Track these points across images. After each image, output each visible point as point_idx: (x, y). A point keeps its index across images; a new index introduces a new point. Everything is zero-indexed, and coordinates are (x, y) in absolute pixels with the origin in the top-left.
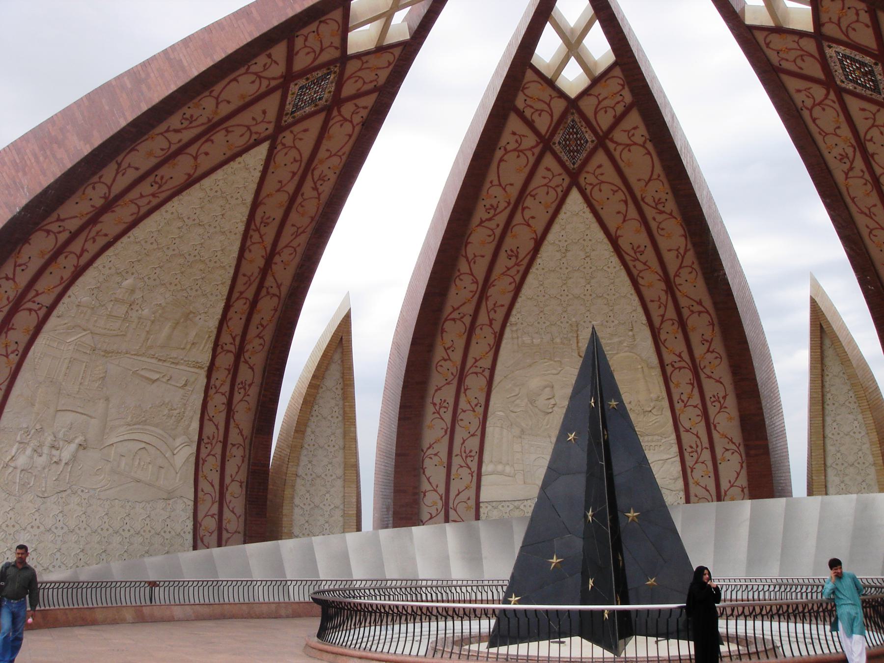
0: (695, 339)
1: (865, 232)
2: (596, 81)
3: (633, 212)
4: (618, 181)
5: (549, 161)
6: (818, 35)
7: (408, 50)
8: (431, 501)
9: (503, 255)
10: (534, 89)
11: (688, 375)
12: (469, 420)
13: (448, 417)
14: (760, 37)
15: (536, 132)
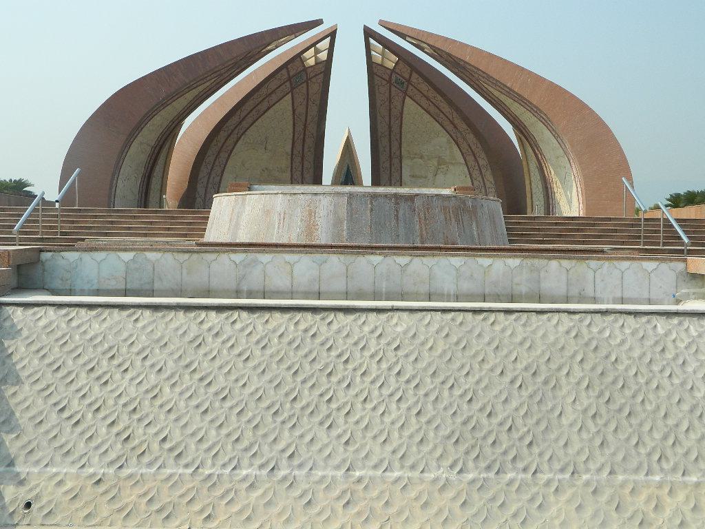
0: (306, 146)
1: (379, 123)
2: (316, 64)
3: (305, 103)
4: (306, 93)
5: (288, 84)
6: (393, 71)
7: (272, 50)
8: (199, 200)
9: (255, 110)
10: (297, 63)
11: (300, 158)
12: (218, 169)
13: (210, 168)
14: (374, 65)
15: (289, 74)
